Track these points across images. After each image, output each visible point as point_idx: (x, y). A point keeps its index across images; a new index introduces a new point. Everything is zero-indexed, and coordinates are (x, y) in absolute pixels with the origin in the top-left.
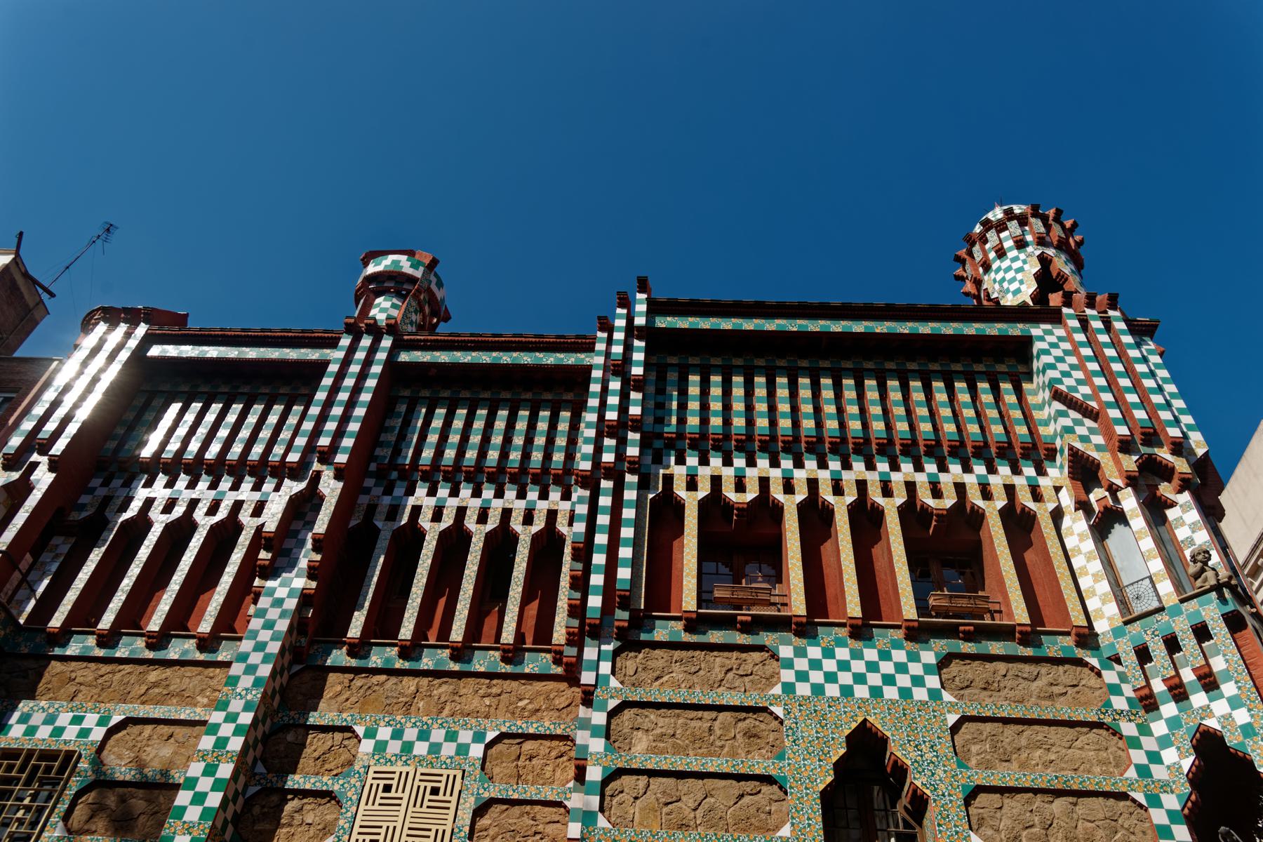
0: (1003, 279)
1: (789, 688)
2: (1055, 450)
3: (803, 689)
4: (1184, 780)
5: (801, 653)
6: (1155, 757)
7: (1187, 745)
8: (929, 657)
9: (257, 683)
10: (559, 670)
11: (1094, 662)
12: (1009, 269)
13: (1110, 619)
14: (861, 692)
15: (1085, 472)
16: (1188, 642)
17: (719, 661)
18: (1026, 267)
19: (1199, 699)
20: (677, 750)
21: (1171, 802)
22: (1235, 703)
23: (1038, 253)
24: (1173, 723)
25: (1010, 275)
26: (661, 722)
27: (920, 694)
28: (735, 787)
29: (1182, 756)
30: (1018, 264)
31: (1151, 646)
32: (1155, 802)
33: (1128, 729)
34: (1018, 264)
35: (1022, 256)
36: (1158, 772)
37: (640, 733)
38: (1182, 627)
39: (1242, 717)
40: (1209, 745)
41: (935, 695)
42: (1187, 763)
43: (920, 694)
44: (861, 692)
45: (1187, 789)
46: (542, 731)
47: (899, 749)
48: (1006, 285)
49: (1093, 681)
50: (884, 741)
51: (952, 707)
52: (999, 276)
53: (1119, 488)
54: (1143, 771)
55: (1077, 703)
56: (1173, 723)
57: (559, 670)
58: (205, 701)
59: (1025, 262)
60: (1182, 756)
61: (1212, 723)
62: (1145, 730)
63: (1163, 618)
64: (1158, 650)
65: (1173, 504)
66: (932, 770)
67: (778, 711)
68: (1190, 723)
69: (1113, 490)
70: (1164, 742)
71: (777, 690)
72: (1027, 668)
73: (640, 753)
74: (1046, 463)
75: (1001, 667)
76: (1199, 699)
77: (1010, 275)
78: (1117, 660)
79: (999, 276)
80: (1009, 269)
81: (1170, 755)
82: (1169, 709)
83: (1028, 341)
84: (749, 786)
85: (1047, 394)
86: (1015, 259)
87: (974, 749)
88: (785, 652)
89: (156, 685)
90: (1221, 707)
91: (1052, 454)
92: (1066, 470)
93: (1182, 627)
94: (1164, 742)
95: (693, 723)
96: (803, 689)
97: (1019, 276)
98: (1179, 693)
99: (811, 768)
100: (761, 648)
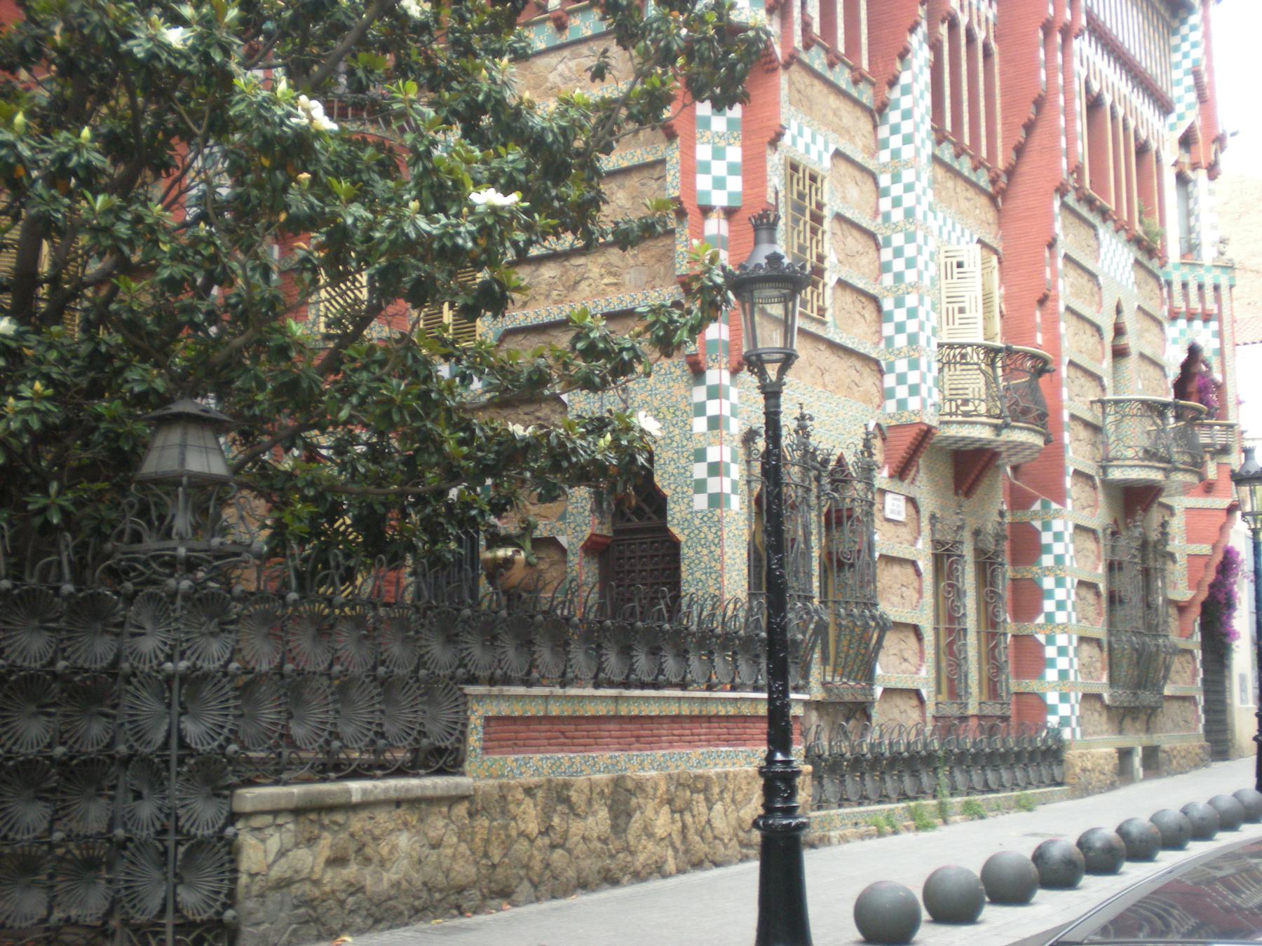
7: (1186, 347)
10: (990, 189)
11: (1163, 280)
15: (1187, 141)
16: (1209, 293)
19: (1198, 324)
24: (1182, 332)
38: (1209, 283)
40: (1194, 351)
42: (1184, 356)
49: (1157, 291)
57: (990, 189)
63: (1202, 271)
76: (1198, 324)
82: (1182, 323)
85: (1187, 64)
93: (1209, 283)
100: (1093, 227)
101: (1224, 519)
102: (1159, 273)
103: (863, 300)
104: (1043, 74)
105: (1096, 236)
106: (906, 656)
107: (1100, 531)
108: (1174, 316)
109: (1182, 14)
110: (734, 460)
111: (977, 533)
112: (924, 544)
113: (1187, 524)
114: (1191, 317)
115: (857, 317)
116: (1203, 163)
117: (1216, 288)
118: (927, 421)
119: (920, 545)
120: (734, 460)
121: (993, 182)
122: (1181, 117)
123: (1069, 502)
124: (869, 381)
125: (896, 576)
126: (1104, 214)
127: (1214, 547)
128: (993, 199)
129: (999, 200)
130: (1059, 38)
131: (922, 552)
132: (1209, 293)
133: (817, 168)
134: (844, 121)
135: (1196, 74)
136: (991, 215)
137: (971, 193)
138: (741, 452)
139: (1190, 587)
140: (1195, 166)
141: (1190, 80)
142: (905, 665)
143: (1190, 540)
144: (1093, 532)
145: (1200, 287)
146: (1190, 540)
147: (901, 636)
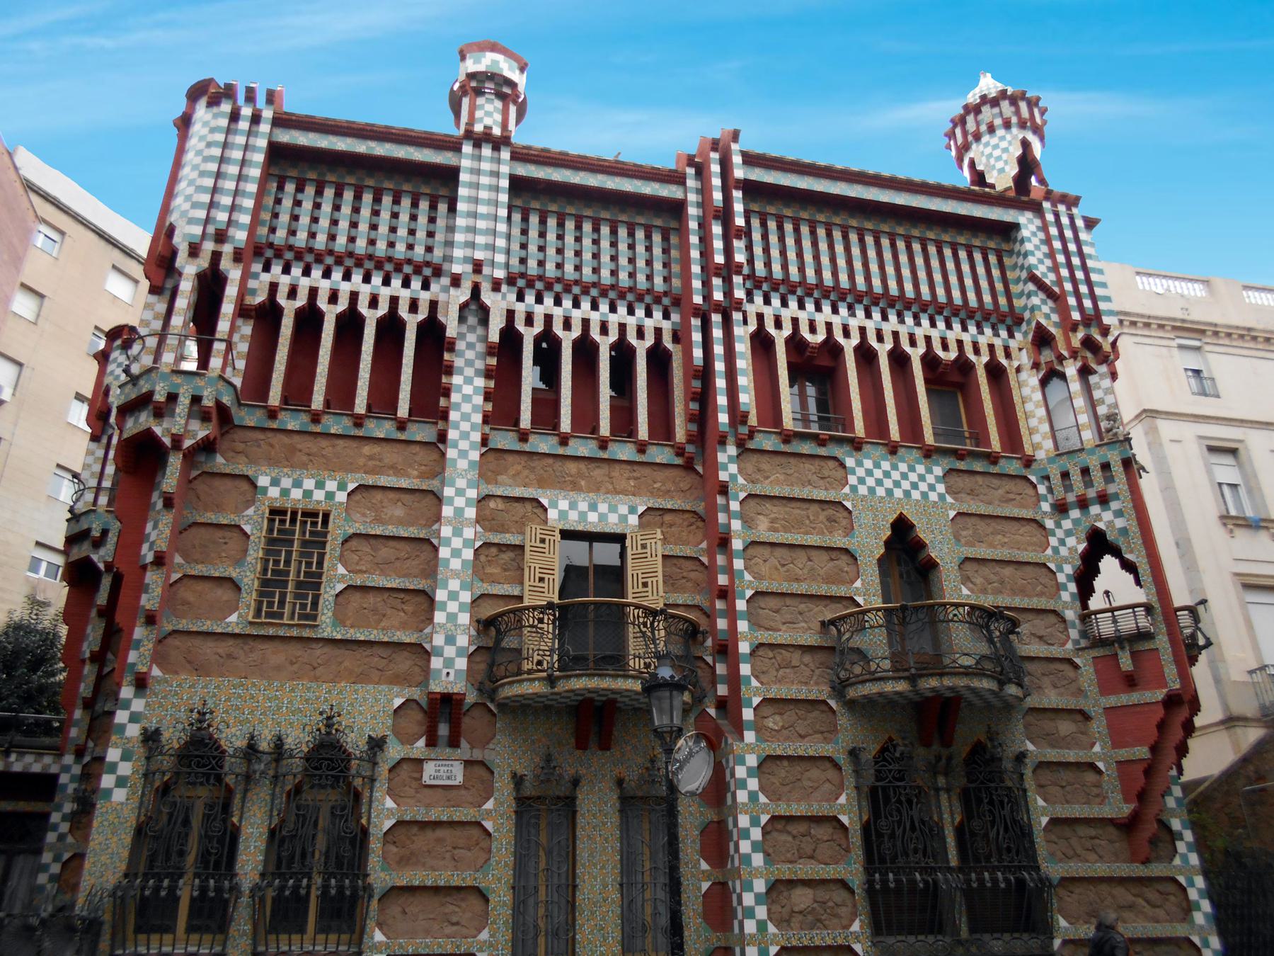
0: (990, 155)
1: (854, 489)
2: (1022, 320)
3: (863, 490)
4: (1077, 557)
5: (860, 464)
6: (1062, 542)
7: (1083, 536)
8: (938, 471)
9: (471, 463)
10: (679, 461)
11: (1033, 479)
12: (996, 147)
13: (1047, 451)
14: (898, 493)
15: (1042, 339)
16: (1097, 474)
17: (808, 466)
18: (1011, 149)
19: (1095, 509)
20: (786, 530)
21: (1068, 569)
22: (1119, 514)
23: (1021, 137)
24: (1075, 522)
25: (997, 153)
26: (775, 509)
27: (933, 496)
28: (824, 556)
29: (1079, 543)
30: (1004, 144)
31: (1072, 472)
32: (1061, 570)
33: (1049, 524)
34: (1004, 144)
35: (1008, 137)
36: (1064, 551)
37: (761, 517)
38: (1094, 462)
39: (1120, 523)
41: (941, 496)
42: (1081, 547)
43: (933, 496)
44: (898, 493)
45: (1079, 563)
46: (676, 507)
47: (922, 533)
48: (992, 161)
49: (1030, 491)
50: (912, 526)
51: (952, 507)
52: (988, 150)
53: (1065, 358)
54: (1056, 550)
55: (1022, 506)
56: (1075, 522)
57: (679, 461)
58: (415, 473)
59: (1010, 143)
60: (1079, 543)
61: (1101, 525)
62: (1058, 525)
63: (1083, 456)
64: (1076, 477)
65: (1095, 372)
66: (942, 546)
67: (848, 504)
68: (1085, 526)
69: (1061, 358)
70: (1068, 533)
71: (847, 490)
72: (996, 482)
73: (762, 531)
74: (1015, 328)
75: (979, 479)
76: (1095, 509)
77: (997, 153)
78: (1047, 478)
79: (988, 150)
80: (996, 147)
81: (1071, 541)
82: (1075, 513)
83: (1015, 227)
84: (834, 554)
85: (1024, 275)
86: (1002, 138)
87: (964, 533)
88: (850, 462)
89: (371, 458)
90: (1107, 516)
91: (1019, 321)
92: (1030, 337)
93: (1094, 462)
94: (1068, 533)
95: (797, 511)
96: (863, 490)
97: (1005, 156)
98: (1083, 504)
99: (870, 542)
100: (835, 458)
101: (1162, 712)
102: (1024, 472)
103: (402, 596)
104: (698, 353)
105: (843, 465)
106: (454, 919)
107: (842, 758)
108: (1061, 509)
109: (1013, 234)
110: (125, 757)
111: (620, 782)
112: (499, 803)
113: (1109, 726)
114: (1083, 504)
115: (389, 611)
116: (1065, 353)
117: (1106, 467)
118: (438, 690)
119: (489, 805)
120: (125, 757)
121: (680, 452)
122: (1029, 322)
123: (750, 736)
124: (404, 663)
125: (439, 840)
126: (857, 445)
127: (1154, 749)
128: (688, 466)
129: (700, 469)
130: (716, 318)
131: (496, 812)
132: (1097, 474)
133: (323, 507)
134: (386, 461)
135: (1033, 278)
136: (686, 481)
137: (647, 471)
138: (140, 751)
139: (1126, 801)
140: (1061, 358)
141: (1031, 287)
142: (449, 930)
143: (1117, 744)
144: (830, 759)
145: (1085, 471)
146: (1117, 744)
147: (448, 899)
